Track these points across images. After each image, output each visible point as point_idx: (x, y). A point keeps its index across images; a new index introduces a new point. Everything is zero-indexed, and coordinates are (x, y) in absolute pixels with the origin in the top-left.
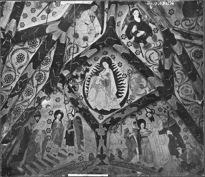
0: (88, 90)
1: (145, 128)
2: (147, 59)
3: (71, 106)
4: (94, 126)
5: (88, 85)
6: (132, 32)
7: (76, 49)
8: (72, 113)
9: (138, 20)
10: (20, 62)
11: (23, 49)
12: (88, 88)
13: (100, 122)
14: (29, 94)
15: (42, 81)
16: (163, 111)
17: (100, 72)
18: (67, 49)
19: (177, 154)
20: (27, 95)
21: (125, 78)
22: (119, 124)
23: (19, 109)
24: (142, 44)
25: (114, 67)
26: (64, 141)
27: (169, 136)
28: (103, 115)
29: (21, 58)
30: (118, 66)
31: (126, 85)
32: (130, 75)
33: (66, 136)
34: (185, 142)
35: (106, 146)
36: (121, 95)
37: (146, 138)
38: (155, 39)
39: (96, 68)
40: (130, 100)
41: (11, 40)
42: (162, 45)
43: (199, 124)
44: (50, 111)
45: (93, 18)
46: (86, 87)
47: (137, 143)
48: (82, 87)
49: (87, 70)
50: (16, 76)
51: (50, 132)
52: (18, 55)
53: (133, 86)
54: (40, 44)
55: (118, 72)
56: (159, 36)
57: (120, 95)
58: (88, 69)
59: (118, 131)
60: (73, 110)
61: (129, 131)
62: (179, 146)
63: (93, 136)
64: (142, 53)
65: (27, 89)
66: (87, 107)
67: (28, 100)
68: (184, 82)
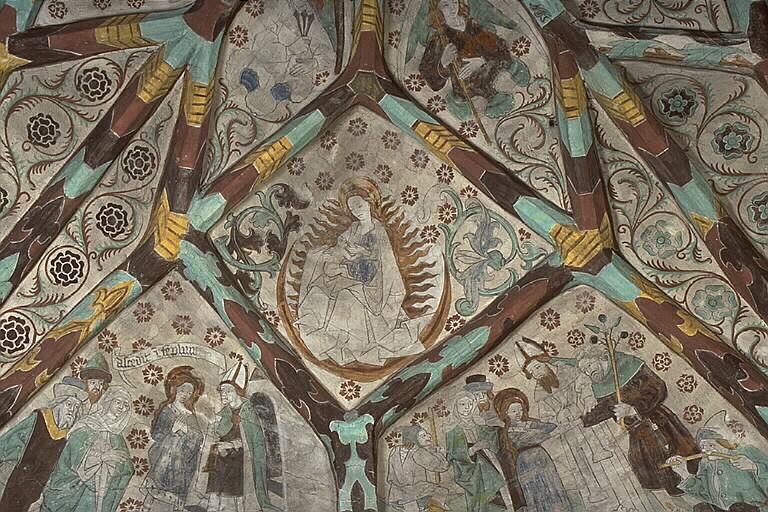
0: (297, 294)
1: (525, 419)
2: (502, 151)
3: (233, 355)
4: (323, 414)
5: (299, 276)
6: (441, 66)
7: (246, 131)
8: (237, 382)
9: (460, 25)
10: (40, 144)
11: (57, 99)
12: (297, 288)
13: (348, 404)
14: (66, 278)
15: (122, 236)
16: (587, 339)
17: (339, 232)
18: (221, 127)
19: (671, 483)
20: (58, 282)
21: (434, 241)
22: (425, 415)
23: (18, 327)
24: (479, 102)
25: (390, 210)
26: (201, 477)
27: (628, 421)
28: (357, 383)
29: (67, 268)
30: (405, 201)
31: (439, 268)
32: (450, 225)
33: (208, 466)
34: (692, 429)
35: (374, 481)
36: (423, 305)
37: (537, 450)
38: (523, 76)
39: (324, 218)
40: (456, 317)
41: (8, 39)
42: (548, 92)
43: (735, 345)
44: (151, 367)
45: (307, 19)
46: (293, 284)
47: (501, 471)
48: (273, 284)
49: (294, 223)
50: (19, 195)
51: (142, 446)
52: (35, 118)
53: (461, 267)
54: (121, 90)
55: (407, 225)
56: (537, 57)
57: (415, 305)
58: (297, 217)
59: (422, 441)
60: (240, 366)
61: (463, 437)
62: (672, 453)
63: (321, 459)
64: (484, 131)
65: (61, 254)
66: (294, 350)
67: (61, 301)
68: (646, 209)
